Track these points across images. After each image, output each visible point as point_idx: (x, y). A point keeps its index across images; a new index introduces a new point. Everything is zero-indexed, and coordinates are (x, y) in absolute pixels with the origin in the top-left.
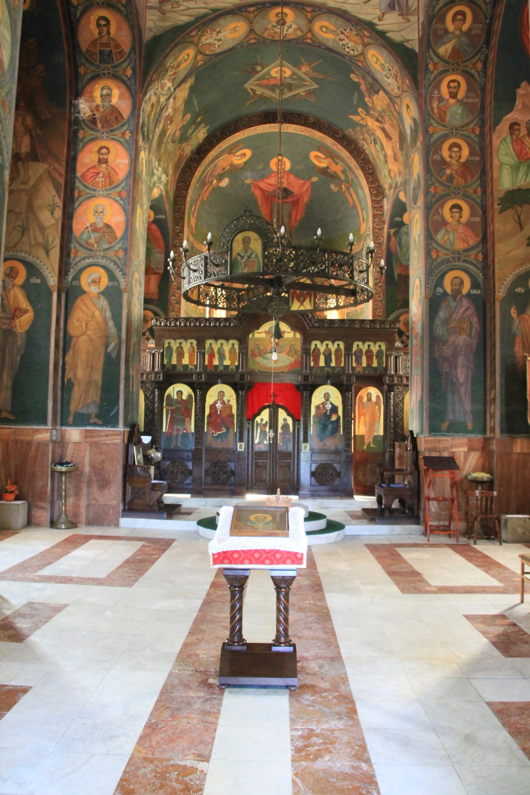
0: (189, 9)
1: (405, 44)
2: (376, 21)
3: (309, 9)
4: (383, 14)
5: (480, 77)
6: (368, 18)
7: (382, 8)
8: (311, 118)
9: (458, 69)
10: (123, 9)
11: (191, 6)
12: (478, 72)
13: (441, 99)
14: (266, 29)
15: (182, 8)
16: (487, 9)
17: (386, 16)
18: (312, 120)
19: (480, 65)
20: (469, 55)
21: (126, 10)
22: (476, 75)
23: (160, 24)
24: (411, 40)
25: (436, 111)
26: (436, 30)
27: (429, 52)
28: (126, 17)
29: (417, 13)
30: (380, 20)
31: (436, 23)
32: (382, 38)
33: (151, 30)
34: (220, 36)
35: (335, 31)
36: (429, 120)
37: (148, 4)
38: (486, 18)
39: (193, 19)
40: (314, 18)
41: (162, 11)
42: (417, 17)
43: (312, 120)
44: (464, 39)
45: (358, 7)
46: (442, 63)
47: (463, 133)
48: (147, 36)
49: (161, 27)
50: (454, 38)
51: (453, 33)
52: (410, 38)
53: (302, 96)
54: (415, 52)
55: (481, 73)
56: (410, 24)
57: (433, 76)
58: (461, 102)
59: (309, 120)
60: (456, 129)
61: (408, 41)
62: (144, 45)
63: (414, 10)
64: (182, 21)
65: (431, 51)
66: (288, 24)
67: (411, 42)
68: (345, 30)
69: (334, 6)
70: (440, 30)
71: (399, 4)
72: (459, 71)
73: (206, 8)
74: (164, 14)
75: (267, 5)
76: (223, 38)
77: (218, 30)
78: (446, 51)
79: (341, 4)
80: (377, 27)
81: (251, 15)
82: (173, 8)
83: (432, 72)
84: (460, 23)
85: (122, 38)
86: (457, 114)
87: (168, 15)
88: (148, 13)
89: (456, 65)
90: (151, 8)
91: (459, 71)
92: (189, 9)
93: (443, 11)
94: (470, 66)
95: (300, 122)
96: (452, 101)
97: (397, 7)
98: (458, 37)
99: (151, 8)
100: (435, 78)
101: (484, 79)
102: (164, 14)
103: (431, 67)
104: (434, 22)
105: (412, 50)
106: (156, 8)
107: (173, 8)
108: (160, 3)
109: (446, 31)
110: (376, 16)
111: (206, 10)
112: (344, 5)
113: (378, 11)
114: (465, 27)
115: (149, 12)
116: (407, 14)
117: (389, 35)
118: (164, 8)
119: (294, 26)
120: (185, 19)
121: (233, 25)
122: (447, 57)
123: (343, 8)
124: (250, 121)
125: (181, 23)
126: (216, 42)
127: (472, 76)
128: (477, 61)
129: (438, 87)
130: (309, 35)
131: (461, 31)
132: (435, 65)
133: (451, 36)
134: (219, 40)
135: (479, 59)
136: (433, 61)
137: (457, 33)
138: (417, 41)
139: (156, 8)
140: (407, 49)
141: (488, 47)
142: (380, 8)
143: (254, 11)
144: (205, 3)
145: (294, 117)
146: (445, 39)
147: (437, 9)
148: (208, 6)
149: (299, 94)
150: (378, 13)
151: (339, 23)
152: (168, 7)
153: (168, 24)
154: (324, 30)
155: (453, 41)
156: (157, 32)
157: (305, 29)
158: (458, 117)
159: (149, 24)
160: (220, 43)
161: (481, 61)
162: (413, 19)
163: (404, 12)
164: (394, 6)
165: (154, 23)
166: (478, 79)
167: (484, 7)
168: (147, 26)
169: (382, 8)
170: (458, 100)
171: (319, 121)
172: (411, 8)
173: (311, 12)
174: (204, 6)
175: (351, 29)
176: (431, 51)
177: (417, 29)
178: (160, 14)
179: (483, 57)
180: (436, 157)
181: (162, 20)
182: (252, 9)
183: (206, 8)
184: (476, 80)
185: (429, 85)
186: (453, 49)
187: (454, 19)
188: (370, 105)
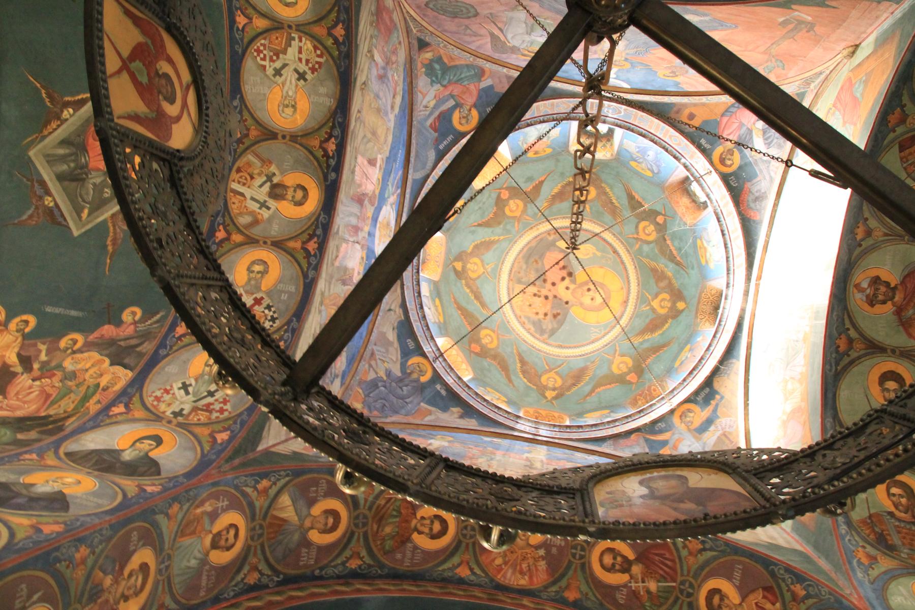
3: (312, 246)
5: (235, 586)
9: (252, 539)
12: (243, 579)
13: (214, 516)
14: (266, 162)
16: (335, 567)
19: (252, 579)
20: (271, 552)
22: (239, 578)
25: (199, 511)
27: (287, 475)
34: (289, 75)
35: (258, 288)
36: (188, 500)
38: (321, 569)
40: (290, 253)
44: (296, 537)
46: (266, 504)
47: (161, 583)
50: (300, 519)
51: (309, 514)
53: (41, 198)
54: (257, 446)
55: (241, 586)
57: (249, 490)
58: (204, 562)
60: (167, 567)
65: (287, 479)
66: (272, 203)
68: (269, 307)
72: (250, 542)
75: (333, 175)
77: (309, 76)
78: (282, 509)
83: (255, 488)
84: (321, 526)
86: (189, 561)
89: (260, 532)
91: (250, 542)
94: (254, 560)
96: (208, 540)
98: (301, 526)
100: (245, 495)
101: (232, 594)
103: (265, 483)
109: (312, 502)
114: (315, 537)
119: (265, 214)
121: (304, 105)
122: (276, 513)
126: (278, 65)
127: (238, 571)
128: (260, 572)
129: (234, 505)
130: (237, 238)
131: (312, 528)
132: (266, 491)
133: (304, 512)
134: (278, 72)
135: (262, 574)
136: (271, 487)
137: (307, 523)
141: (280, 584)
143: (325, 150)
146: (301, 503)
149: (48, 193)
151: (284, 297)
154: (257, 268)
155: (296, 518)
157: (256, 232)
158: (185, 563)
160: (270, 71)
161: (259, 580)
166: (233, 583)
167: (339, 561)
170: (207, 554)
173: (306, 251)
175: (273, 319)
176: (287, 479)
179: (265, 580)
180: (135, 536)
182: (331, 147)
184: (233, 579)
185: (237, 487)
186: (284, 521)
187: (335, 514)
188: (63, 343)
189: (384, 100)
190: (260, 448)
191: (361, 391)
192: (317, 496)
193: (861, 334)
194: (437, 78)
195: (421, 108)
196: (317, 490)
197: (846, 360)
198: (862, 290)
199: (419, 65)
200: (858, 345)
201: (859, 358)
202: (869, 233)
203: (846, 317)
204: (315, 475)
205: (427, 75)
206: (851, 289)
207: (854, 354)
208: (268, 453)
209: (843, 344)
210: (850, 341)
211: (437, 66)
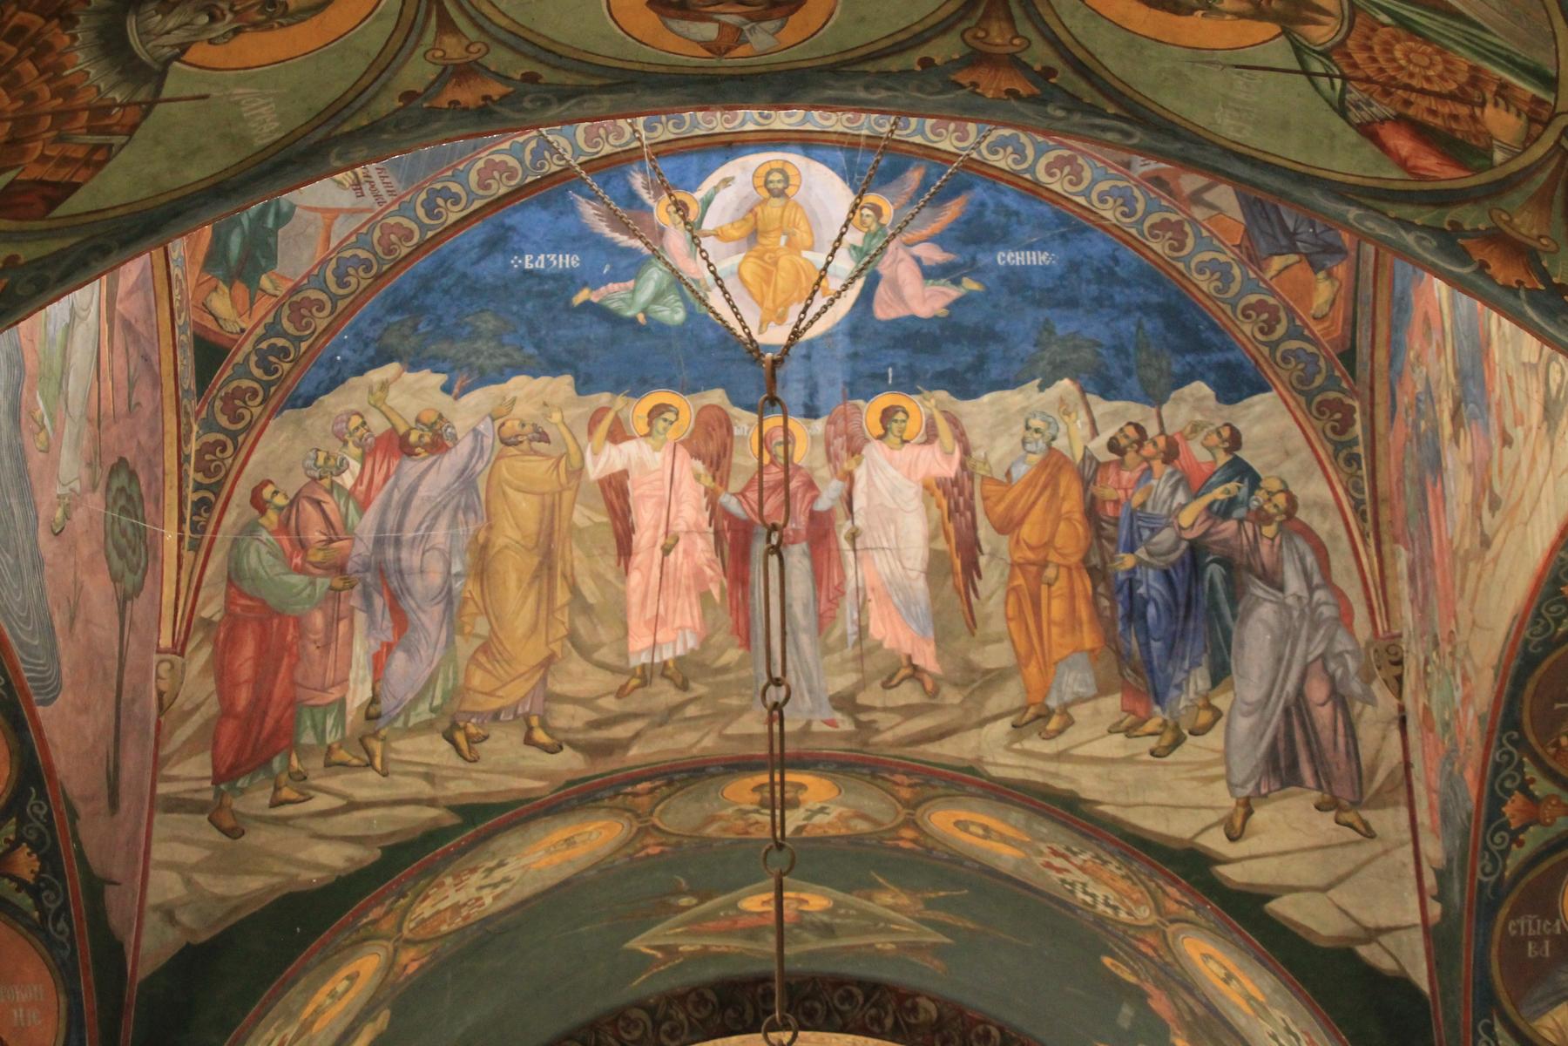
0: (352, 806)
1: (1363, 951)
2: (1215, 842)
4: (1247, 807)
6: (1179, 828)
7: (1238, 777)
8: (922, 1001)
10: (25, 901)
11: (362, 794)
15: (321, 802)
17: (1261, 815)
18: (929, 1009)
21: (38, 904)
23: (219, 886)
24: (1389, 930)
26: (1520, 942)
27: (1489, 1029)
28: (38, 930)
29: (1403, 790)
30: (1232, 839)
31: (1515, 914)
32: (1247, 915)
33: (169, 914)
37: (162, 789)
39: (367, 855)
41: (228, 823)
42: (1403, 814)
43: (929, 1009)
45: (1127, 774)
48: (152, 947)
49: (222, 899)
52: (1384, 922)
56: (1376, 847)
59: (914, 1009)
61: (1373, 934)
62: (132, 993)
63: (1391, 774)
64: (317, 866)
65: (1498, 1029)
67: (1385, 939)
69: (1018, 774)
70: (1538, 940)
71: (1316, 758)
73: (432, 802)
74: (234, 833)
76: (517, 875)
79: (1052, 767)
80: (1223, 870)
81: (645, 800)
82: (275, 804)
85: (17, 1014)
87: (258, 837)
88: (158, 831)
90: (176, 805)
92: (352, 806)
93: (1545, 865)
95: (878, 1021)
97: (1306, 771)
99: (176, 805)
102: (234, 833)
104: (1504, 912)
105: (1401, 984)
106: (199, 808)
107: (274, 805)
108: (217, 779)
110: (1212, 817)
111: (431, 813)
112: (1065, 768)
113: (1221, 786)
115: (164, 824)
116: (1356, 804)
117: (1281, 907)
118: (238, 804)
120: (333, 858)
123: (1062, 785)
124: (657, 1024)
125: (313, 877)
138: (1418, 935)
139: (199, 808)
140: (1371, 974)
142: (1228, 777)
144: (429, 777)
145: (849, 997)
147: (1512, 863)
148: (439, 793)
149: (871, 945)
150: (1224, 799)
152: (255, 799)
153: (251, 884)
156: (197, 927)
159: (165, 886)
162: (1389, 821)
163: (1345, 792)
164: (1294, 764)
165: (188, 882)
168: (153, 898)
169: (1238, 777)
171: (960, 1011)
172: (1373, 771)
174: (425, 789)
176: (1498, 1029)
177: (1411, 884)
178: (215, 836)
181: (225, 864)
182: (646, 785)
183: (432, 802)
189: (440, 535)
190: (1425, 987)
191: (1277, 263)
192: (1553, 937)
193: (943, 28)
194: (262, 214)
195: (369, 200)
196: (1533, 938)
197: (1066, 77)
198: (736, 37)
199: (263, 306)
200: (998, 36)
201: (1054, 42)
202: (465, 71)
203: (868, 67)
204: (1494, 950)
205: (272, 257)
206: (738, 59)
207: (1040, 55)
208: (1439, 939)
209: (992, 84)
210: (976, 58)
211: (235, 242)
